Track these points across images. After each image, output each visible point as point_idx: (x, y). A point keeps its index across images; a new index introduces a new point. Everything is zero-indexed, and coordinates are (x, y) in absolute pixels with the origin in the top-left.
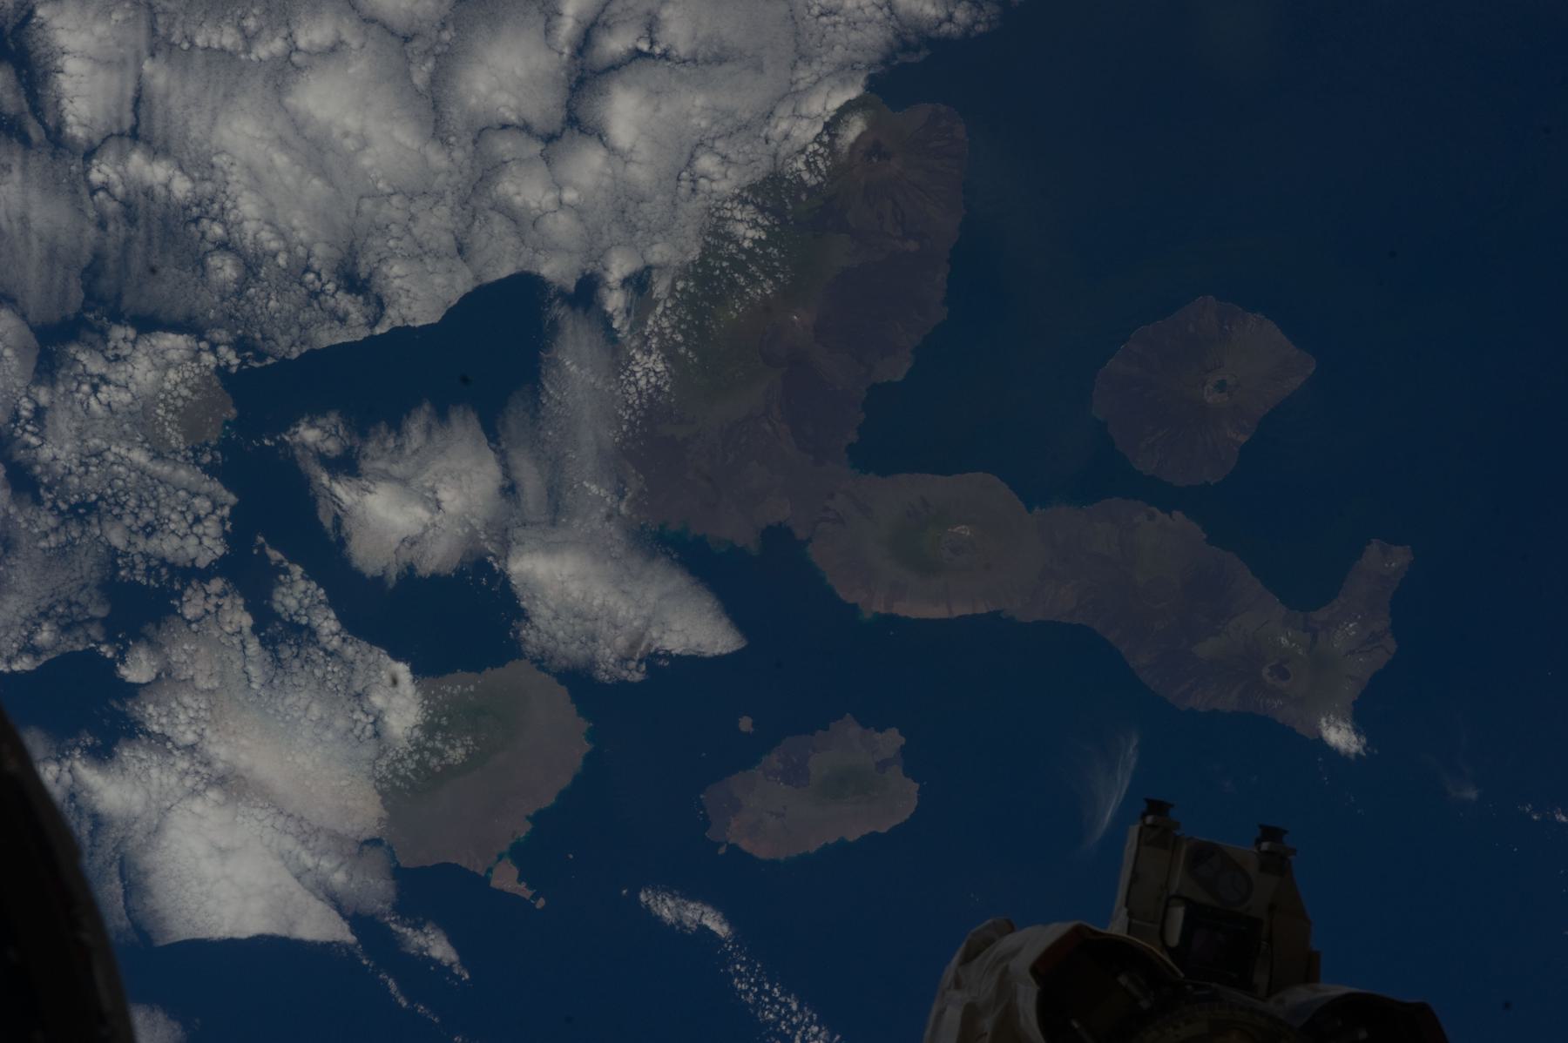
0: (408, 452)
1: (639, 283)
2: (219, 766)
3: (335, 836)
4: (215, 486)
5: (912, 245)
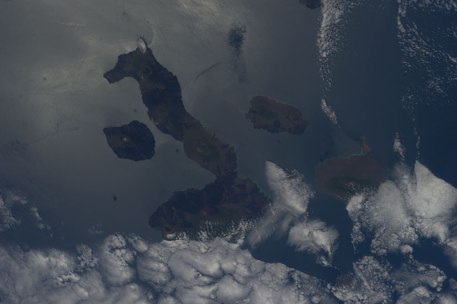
0: (307, 246)
1: (233, 241)
2: (410, 219)
3: (397, 186)
4: (355, 267)
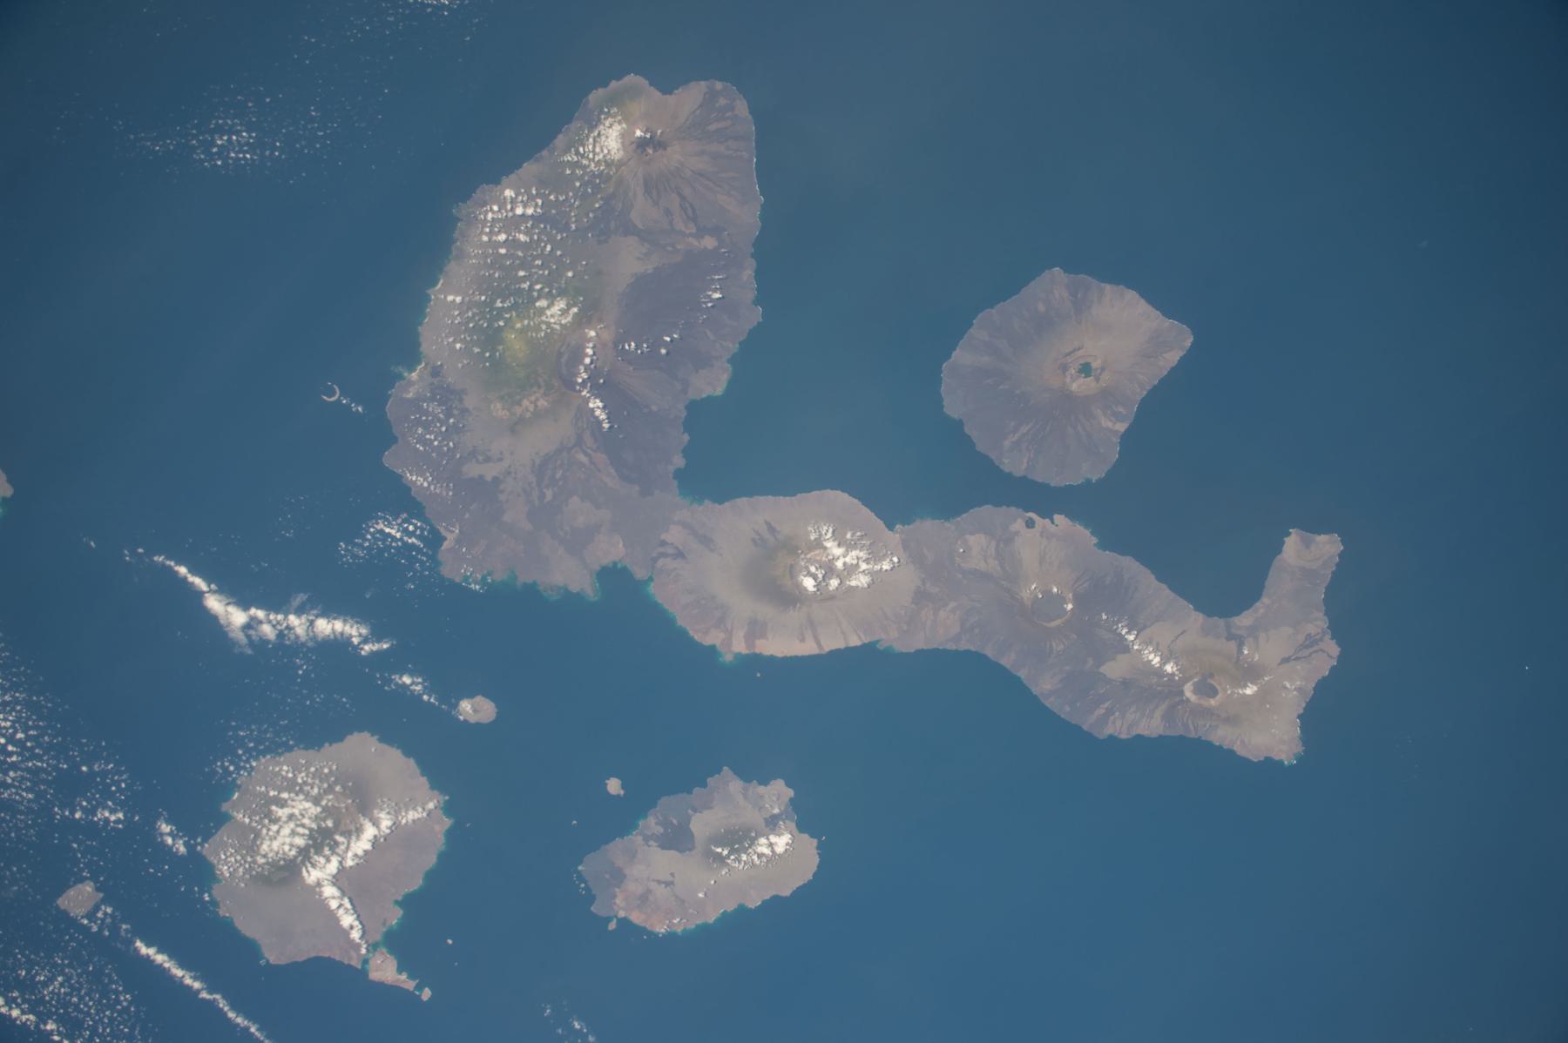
5: (709, 242)
